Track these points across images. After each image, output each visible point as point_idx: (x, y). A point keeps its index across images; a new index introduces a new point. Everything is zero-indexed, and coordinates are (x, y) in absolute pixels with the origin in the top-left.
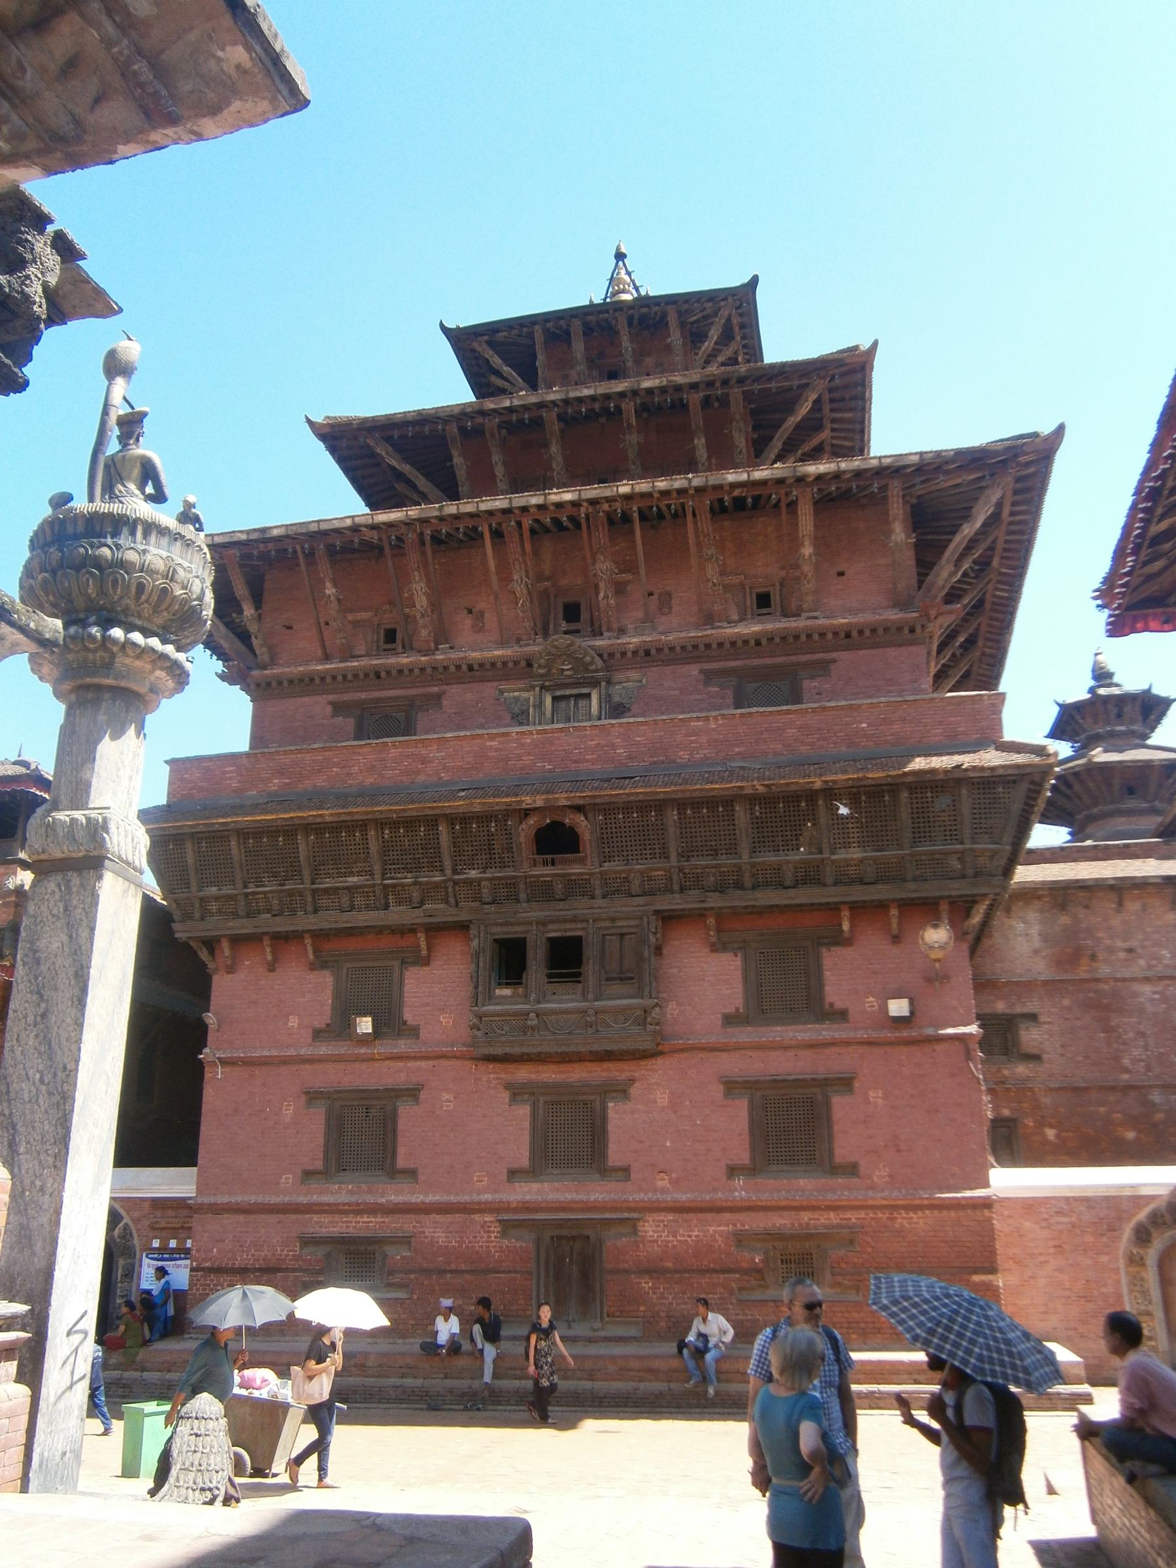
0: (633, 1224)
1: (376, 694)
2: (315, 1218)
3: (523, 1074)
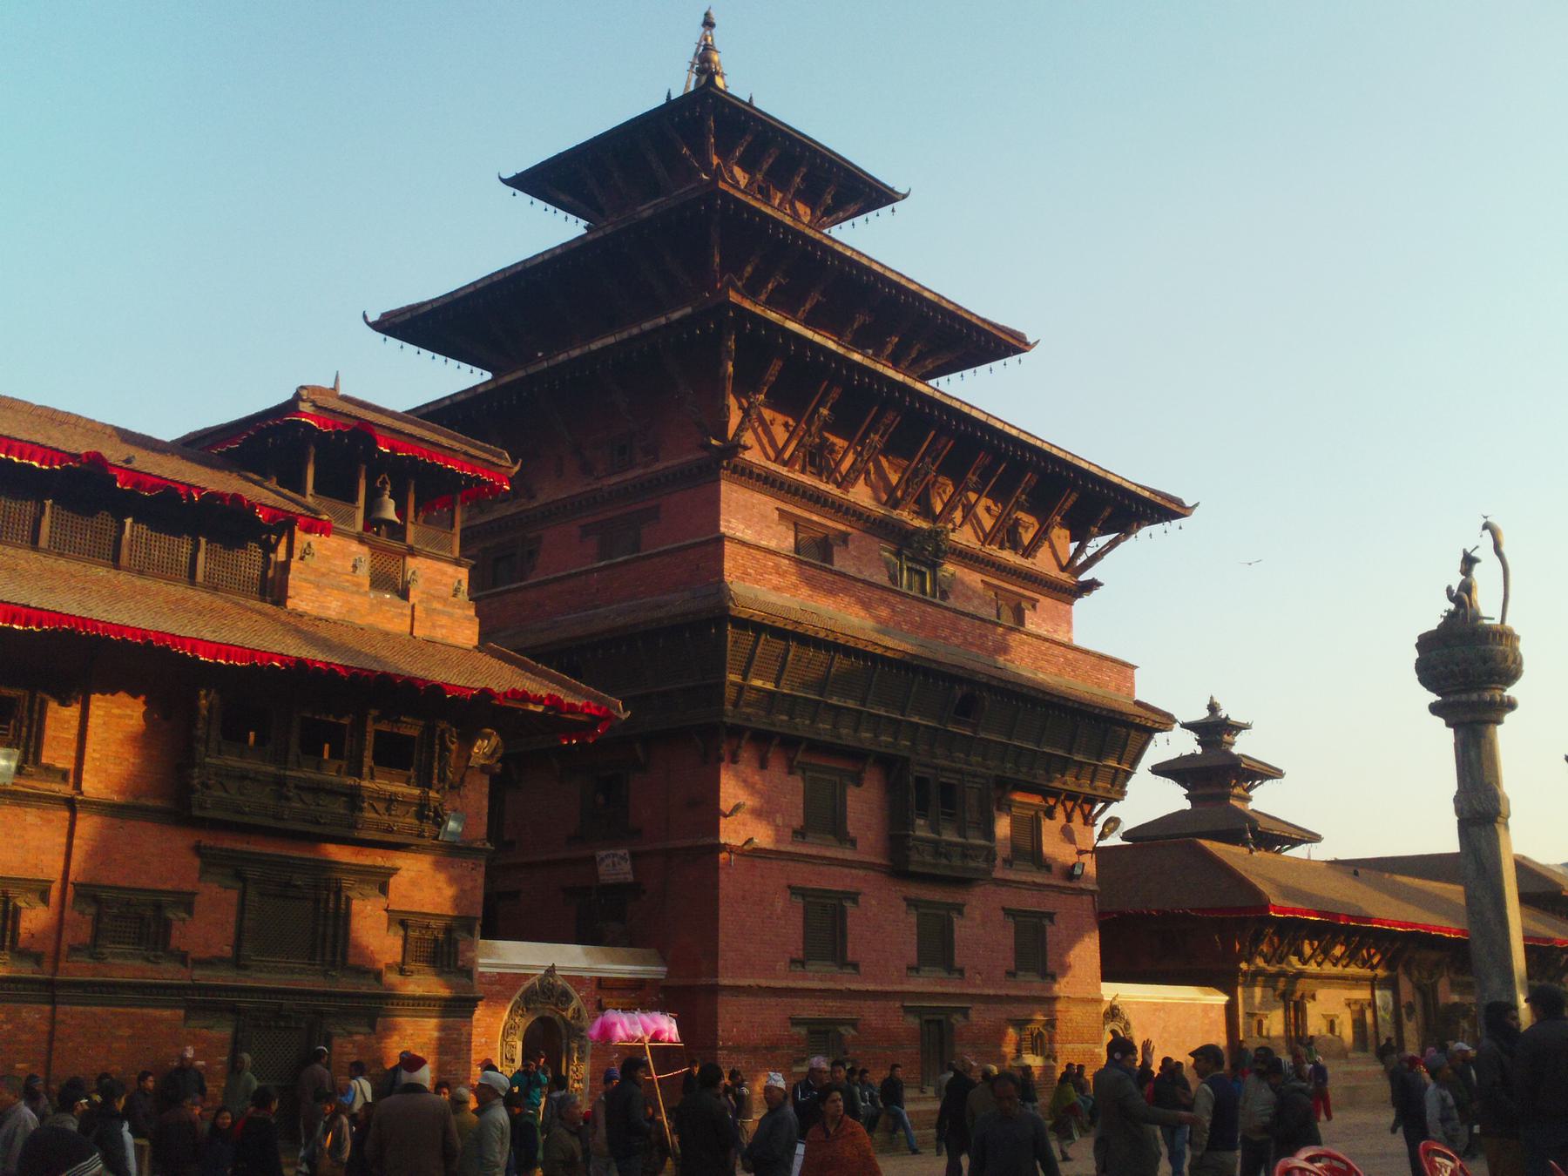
0: (965, 1012)
1: (806, 515)
2: (799, 1001)
3: (915, 891)
